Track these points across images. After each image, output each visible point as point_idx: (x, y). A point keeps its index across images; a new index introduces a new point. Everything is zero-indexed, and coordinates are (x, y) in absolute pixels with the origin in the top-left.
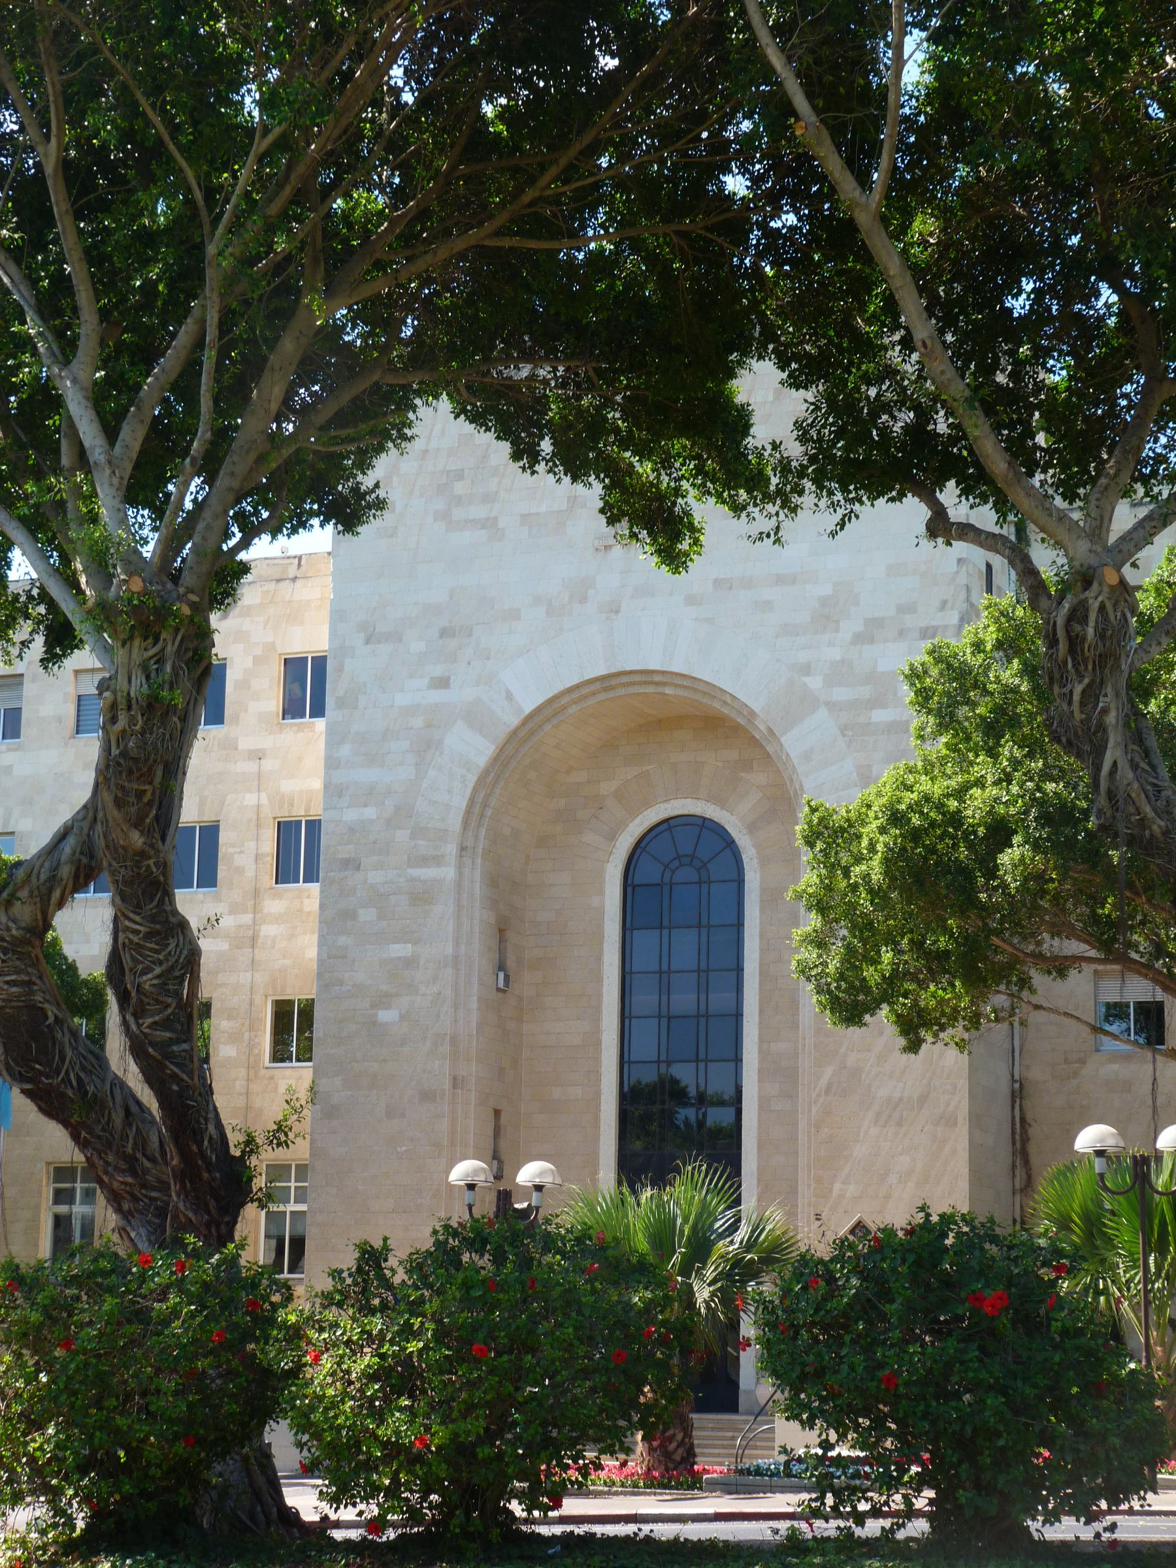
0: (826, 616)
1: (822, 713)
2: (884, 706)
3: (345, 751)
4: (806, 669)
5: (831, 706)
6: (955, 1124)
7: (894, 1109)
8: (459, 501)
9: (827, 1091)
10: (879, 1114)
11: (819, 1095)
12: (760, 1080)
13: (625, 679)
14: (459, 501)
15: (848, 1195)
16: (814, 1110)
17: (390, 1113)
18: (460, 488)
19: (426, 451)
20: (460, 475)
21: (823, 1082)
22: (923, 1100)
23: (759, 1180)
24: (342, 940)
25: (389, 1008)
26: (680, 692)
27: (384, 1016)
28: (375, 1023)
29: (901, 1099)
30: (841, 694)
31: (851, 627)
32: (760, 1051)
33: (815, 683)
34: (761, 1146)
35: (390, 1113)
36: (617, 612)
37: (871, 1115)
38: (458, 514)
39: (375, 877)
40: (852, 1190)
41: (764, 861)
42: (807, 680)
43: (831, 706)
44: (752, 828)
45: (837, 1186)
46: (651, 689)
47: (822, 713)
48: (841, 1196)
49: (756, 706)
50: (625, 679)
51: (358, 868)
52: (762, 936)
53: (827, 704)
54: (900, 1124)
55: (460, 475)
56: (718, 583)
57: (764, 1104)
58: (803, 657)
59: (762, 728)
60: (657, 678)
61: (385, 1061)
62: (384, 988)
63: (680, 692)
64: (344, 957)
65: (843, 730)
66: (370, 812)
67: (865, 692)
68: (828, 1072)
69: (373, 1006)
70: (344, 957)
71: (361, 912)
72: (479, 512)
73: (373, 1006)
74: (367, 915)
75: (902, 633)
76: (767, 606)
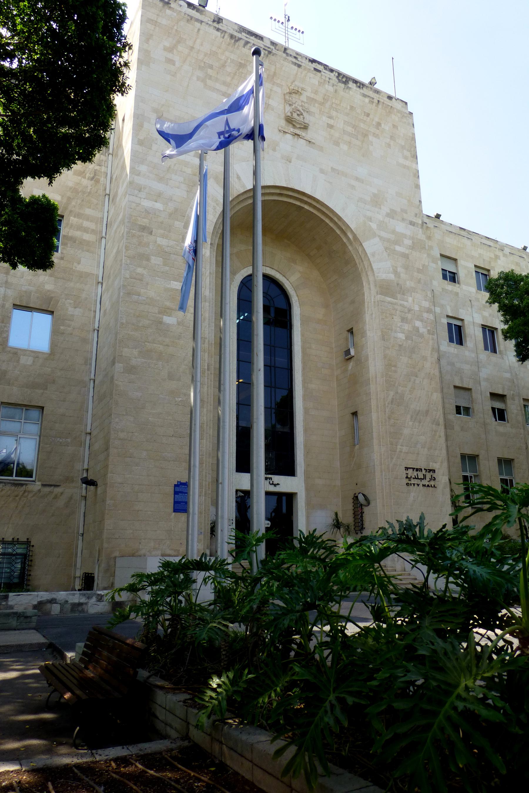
0: (377, 200)
1: (377, 240)
2: (400, 246)
3: (143, 168)
4: (370, 219)
5: (381, 238)
6: (439, 425)
7: (417, 415)
8: (210, 77)
9: (392, 402)
10: (412, 417)
11: (388, 404)
12: (304, 400)
13: (290, 193)
14: (210, 77)
15: (403, 451)
16: (387, 410)
17: (171, 377)
18: (210, 71)
19: (192, 48)
20: (211, 67)
21: (390, 398)
22: (427, 412)
23: (305, 446)
24: (140, 270)
25: (170, 316)
26: (311, 210)
27: (168, 320)
28: (161, 323)
29: (419, 411)
30: (383, 234)
31: (385, 209)
32: (304, 386)
33: (374, 226)
34: (306, 430)
35: (171, 377)
36: (290, 162)
37: (409, 416)
38: (209, 82)
39: (160, 241)
40: (405, 449)
41: (301, 304)
42: (370, 223)
43: (381, 238)
44: (296, 289)
45: (399, 447)
46: (298, 203)
47: (377, 240)
48: (401, 452)
49: (353, 226)
50: (290, 193)
51: (151, 233)
52: (302, 335)
53: (379, 236)
54: (420, 422)
55: (211, 67)
56: (332, 169)
57: (306, 411)
58: (369, 214)
59: (351, 236)
60: (305, 199)
61: (168, 345)
62: (168, 304)
63: (311, 210)
64: (141, 280)
65: (386, 249)
66: (159, 206)
67: (392, 237)
68: (392, 393)
69: (160, 313)
70: (141, 280)
71: (153, 257)
72: (223, 88)
73: (160, 313)
74: (156, 261)
75: (403, 220)
76: (353, 187)
